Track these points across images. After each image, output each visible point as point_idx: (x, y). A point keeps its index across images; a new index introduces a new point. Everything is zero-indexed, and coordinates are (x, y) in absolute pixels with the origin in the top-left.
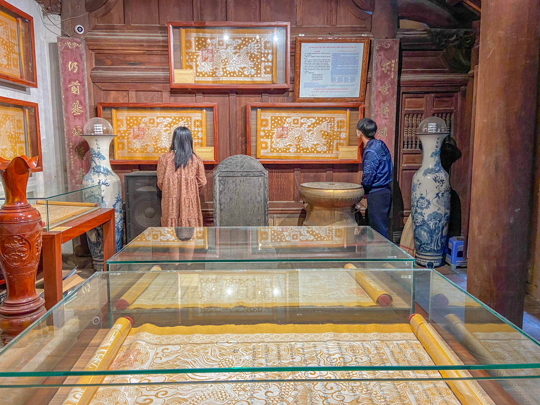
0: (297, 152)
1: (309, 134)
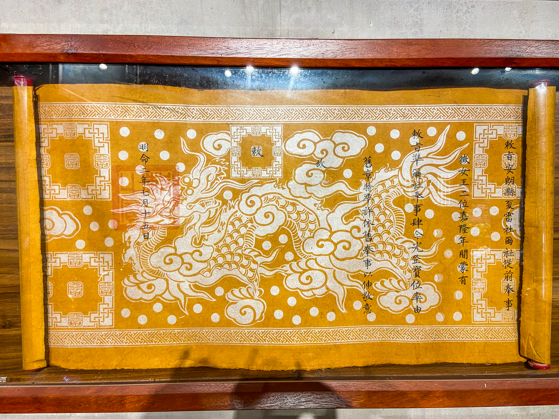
0: (268, 320)
1: (336, 218)
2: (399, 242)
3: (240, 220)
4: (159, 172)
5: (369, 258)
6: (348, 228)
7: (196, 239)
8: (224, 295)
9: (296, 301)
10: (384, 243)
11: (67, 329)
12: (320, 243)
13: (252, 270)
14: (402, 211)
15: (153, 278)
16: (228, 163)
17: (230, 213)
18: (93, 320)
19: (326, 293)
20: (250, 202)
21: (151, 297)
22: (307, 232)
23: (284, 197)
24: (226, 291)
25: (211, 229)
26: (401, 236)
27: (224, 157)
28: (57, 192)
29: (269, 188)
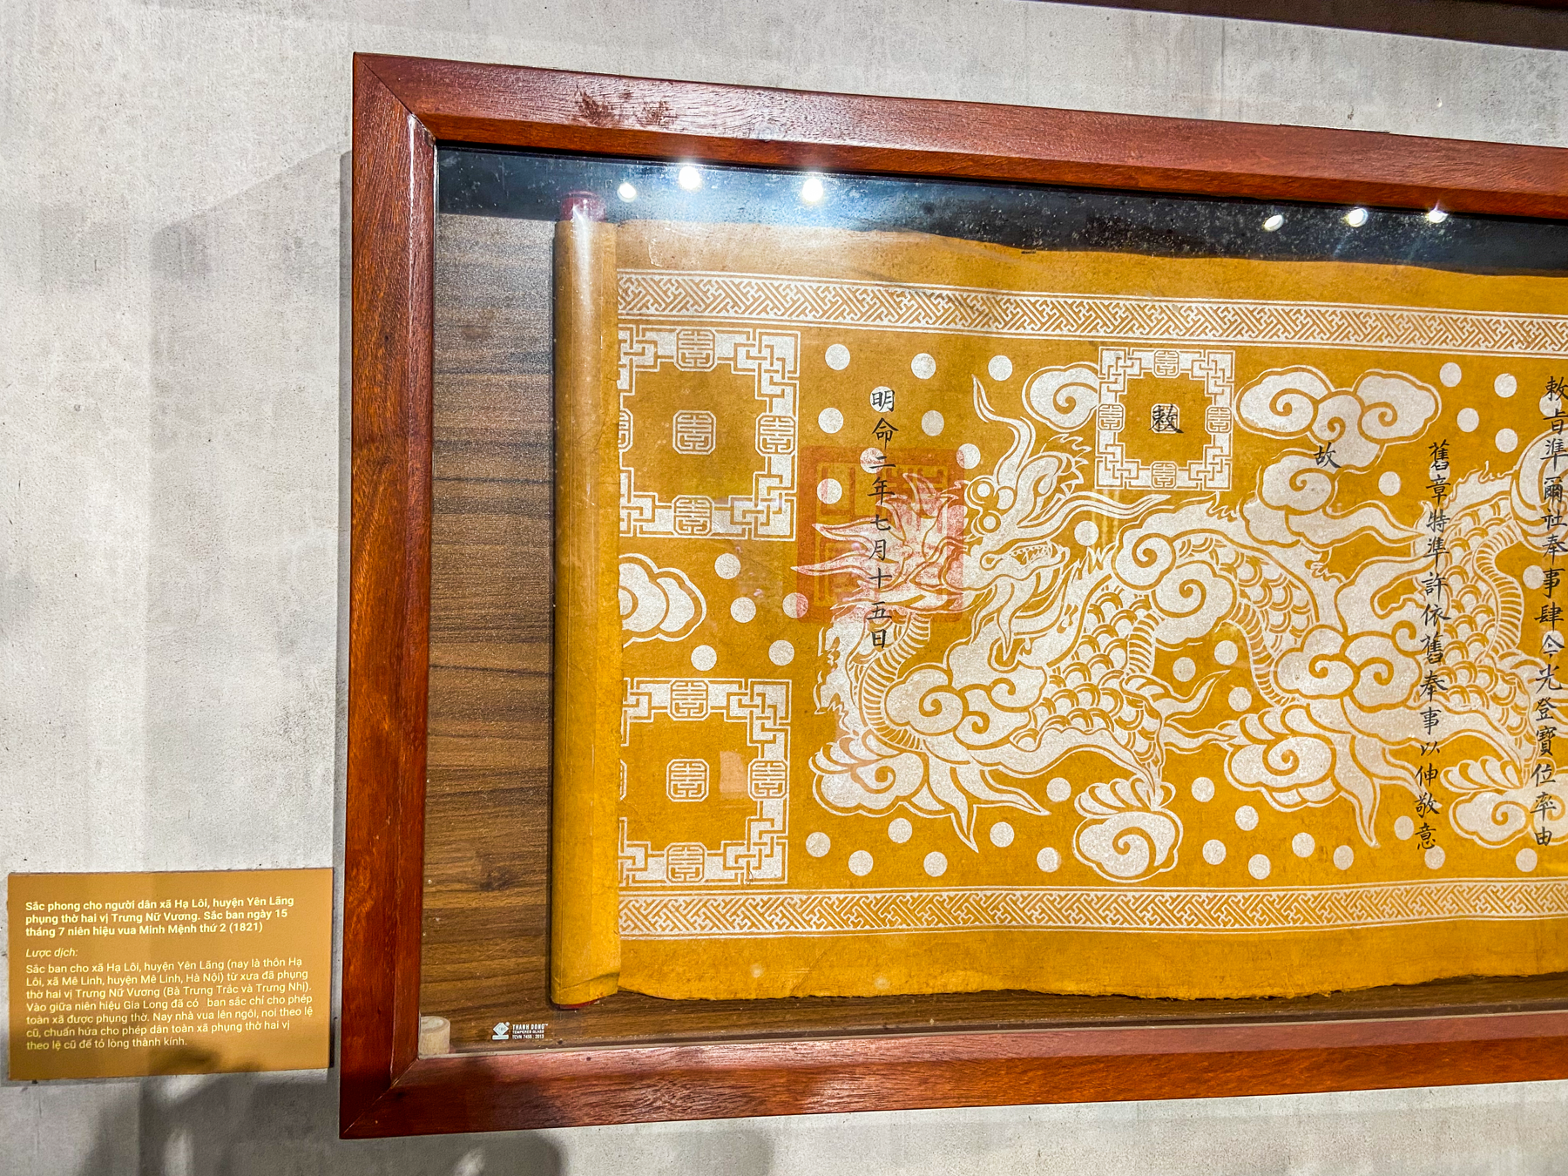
0: (1186, 869)
2: (1505, 665)
3: (1115, 599)
4: (916, 468)
5: (1435, 706)
6: (1386, 626)
7: (1000, 647)
8: (1071, 800)
9: (1256, 818)
10: (1470, 667)
11: (664, 888)
12: (1318, 666)
13: (1145, 734)
14: (1516, 584)
15: (886, 751)
16: (1088, 449)
17: (1090, 580)
18: (731, 863)
19: (1333, 796)
20: (1145, 552)
21: (883, 801)
22: (1287, 635)
23: (1231, 541)
24: (1076, 791)
25: (1044, 621)
26: (1514, 649)
27: (1078, 433)
28: (648, 514)
29: (1194, 516)
